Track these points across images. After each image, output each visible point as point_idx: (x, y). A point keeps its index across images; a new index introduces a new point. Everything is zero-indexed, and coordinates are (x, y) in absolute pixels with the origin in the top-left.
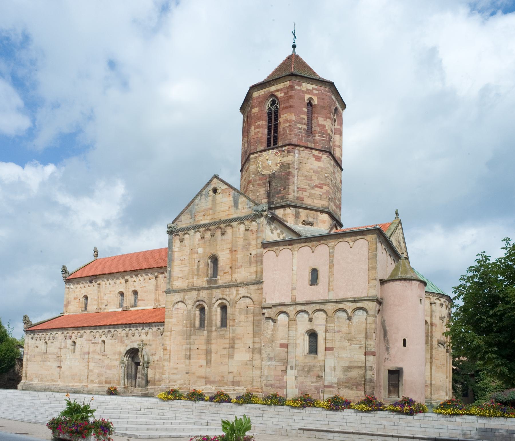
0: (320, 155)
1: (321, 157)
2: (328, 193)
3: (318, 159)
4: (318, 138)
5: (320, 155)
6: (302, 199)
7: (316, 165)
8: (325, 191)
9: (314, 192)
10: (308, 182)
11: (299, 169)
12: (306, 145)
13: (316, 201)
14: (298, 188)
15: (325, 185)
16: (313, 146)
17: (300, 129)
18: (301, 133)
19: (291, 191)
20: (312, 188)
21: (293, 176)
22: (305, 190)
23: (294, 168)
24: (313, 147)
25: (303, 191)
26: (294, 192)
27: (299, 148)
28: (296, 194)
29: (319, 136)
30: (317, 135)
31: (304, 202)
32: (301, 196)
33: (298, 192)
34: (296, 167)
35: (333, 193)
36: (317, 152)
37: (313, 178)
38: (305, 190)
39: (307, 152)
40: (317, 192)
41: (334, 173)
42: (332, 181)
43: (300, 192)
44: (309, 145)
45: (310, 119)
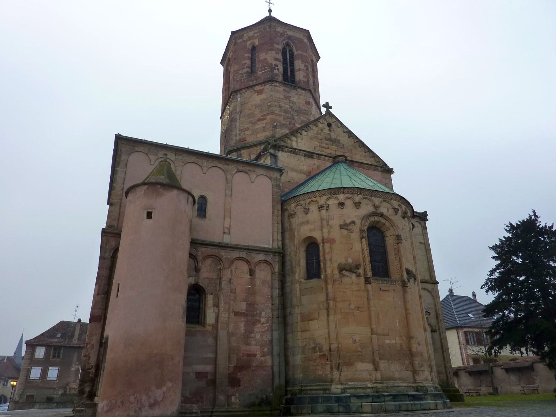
0: (262, 88)
1: (264, 89)
2: (273, 121)
3: (260, 92)
4: (259, 73)
5: (262, 88)
6: (245, 140)
7: (257, 99)
8: (269, 121)
9: (256, 127)
10: (250, 119)
11: (241, 112)
12: (247, 86)
13: (259, 135)
14: (240, 130)
15: (268, 114)
16: (255, 82)
17: (242, 74)
18: (243, 77)
19: (233, 137)
20: (255, 123)
21: (236, 121)
22: (248, 129)
23: (236, 113)
24: (255, 84)
25: (245, 131)
26: (236, 136)
27: (241, 92)
28: (238, 138)
29: (261, 71)
30: (258, 71)
31: (246, 142)
32: (244, 137)
33: (240, 134)
34: (238, 111)
35: (285, 119)
36: (260, 86)
37: (255, 113)
38: (248, 129)
39: (249, 91)
40: (260, 125)
41: (287, 98)
42: (280, 107)
43: (242, 134)
44: (251, 84)
45: (252, 60)
